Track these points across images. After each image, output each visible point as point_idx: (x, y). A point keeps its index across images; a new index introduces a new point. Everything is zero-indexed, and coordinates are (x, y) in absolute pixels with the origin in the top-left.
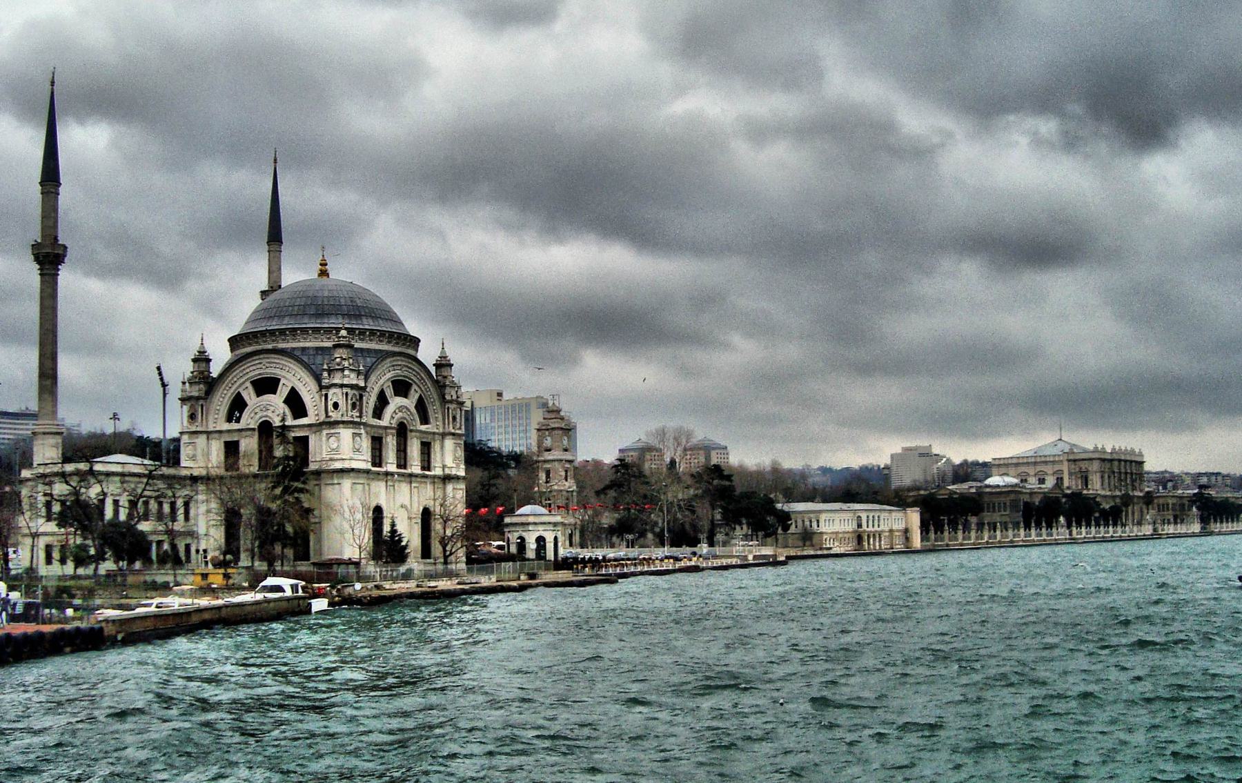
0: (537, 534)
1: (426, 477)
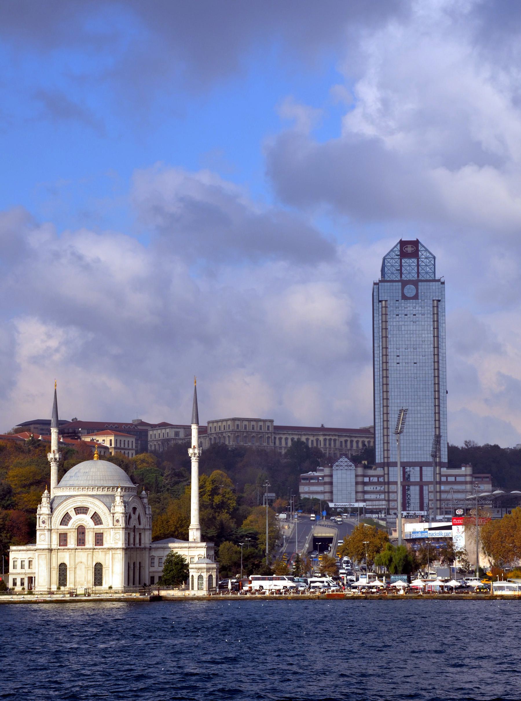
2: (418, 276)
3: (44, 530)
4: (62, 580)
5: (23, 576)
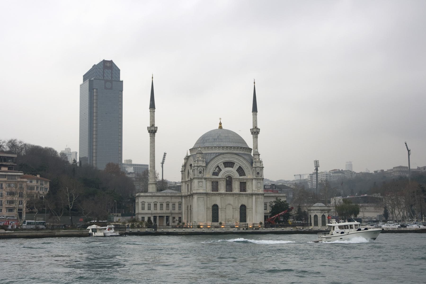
0: (314, 214)
1: (242, 194)
2: (112, 79)
3: (202, 178)
4: (215, 218)
5: (149, 216)
